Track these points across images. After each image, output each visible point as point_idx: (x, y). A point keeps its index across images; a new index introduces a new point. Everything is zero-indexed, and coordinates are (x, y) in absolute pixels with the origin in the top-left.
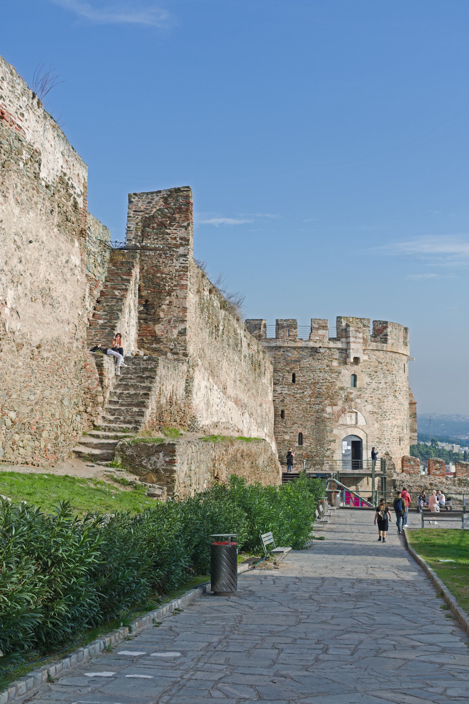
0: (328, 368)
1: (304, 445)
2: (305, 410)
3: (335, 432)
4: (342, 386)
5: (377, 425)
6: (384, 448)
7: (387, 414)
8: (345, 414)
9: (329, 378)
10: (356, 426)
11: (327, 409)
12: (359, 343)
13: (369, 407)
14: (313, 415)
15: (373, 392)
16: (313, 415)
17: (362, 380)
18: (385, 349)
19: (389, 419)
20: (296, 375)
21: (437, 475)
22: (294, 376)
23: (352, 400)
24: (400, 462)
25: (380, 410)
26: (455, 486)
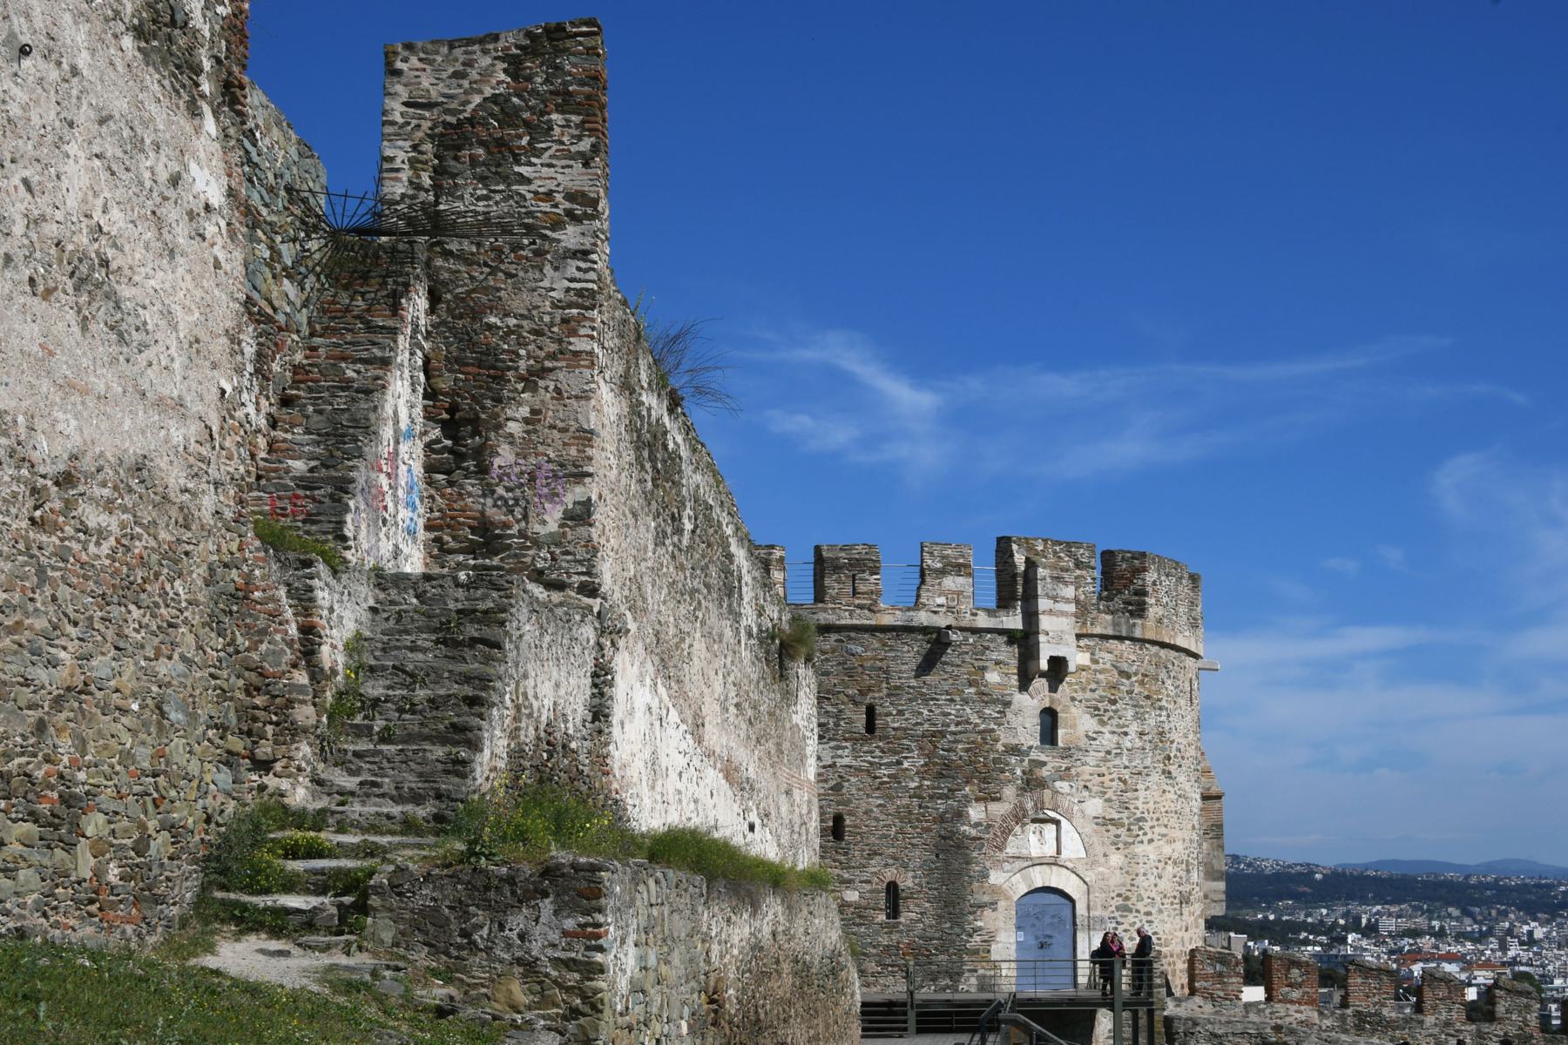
0: (972, 690)
1: (902, 920)
2: (905, 816)
3: (996, 878)
5: (1116, 859)
7: (1147, 826)
8: (1024, 824)
9: (975, 719)
10: (1054, 862)
11: (971, 811)
12: (1063, 614)
13: (1095, 806)
14: (928, 830)
15: (1105, 761)
16: (928, 830)
17: (1074, 726)
18: (1138, 633)
19: (1150, 841)
21: (1292, 1002)
22: (871, 712)
23: (1042, 784)
24: (1182, 966)
26: (1345, 1031)
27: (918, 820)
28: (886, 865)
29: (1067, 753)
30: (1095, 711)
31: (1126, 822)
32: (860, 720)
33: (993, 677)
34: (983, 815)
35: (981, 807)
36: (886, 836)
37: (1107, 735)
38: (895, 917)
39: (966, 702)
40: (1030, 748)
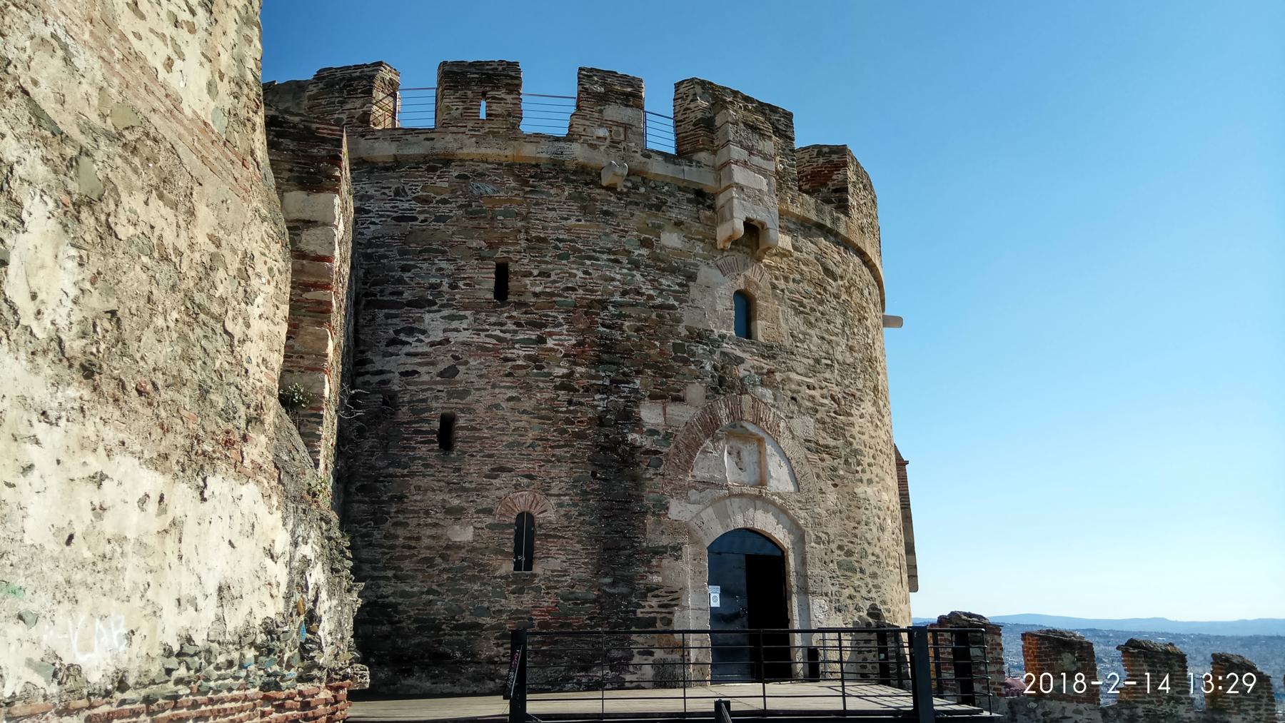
0: (645, 252)
2: (546, 414)
3: (678, 510)
4: (700, 326)
8: (716, 439)
9: (647, 289)
14: (580, 436)
16: (580, 436)
20: (513, 267)
22: (502, 273)
27: (568, 422)
28: (517, 487)
29: (769, 351)
30: (798, 308)
32: (488, 281)
34: (660, 420)
36: (519, 444)
38: (529, 567)
39: (636, 265)
40: (723, 337)
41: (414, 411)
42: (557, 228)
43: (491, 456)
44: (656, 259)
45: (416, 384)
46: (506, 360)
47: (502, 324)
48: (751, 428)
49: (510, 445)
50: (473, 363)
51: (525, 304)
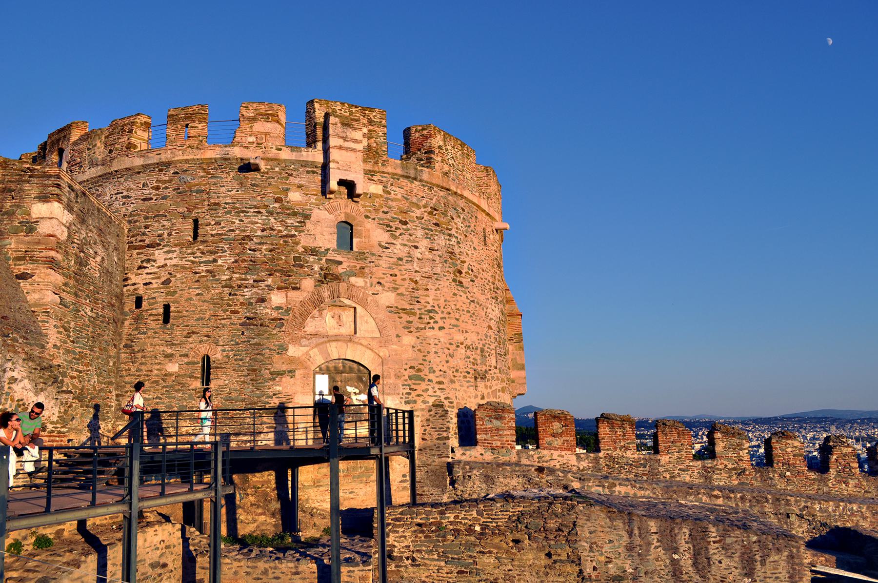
0: (277, 205)
2: (217, 302)
3: (293, 351)
4: (312, 245)
5: (408, 339)
6: (430, 392)
7: (437, 317)
10: (350, 339)
11: (273, 297)
13: (387, 298)
19: (441, 328)
21: (555, 449)
25: (418, 306)
29: (361, 256)
31: (418, 312)
33: (295, 196)
34: (284, 301)
35: (282, 294)
36: (202, 319)
37: (399, 246)
38: (208, 382)
40: (328, 250)
41: (150, 304)
42: (225, 197)
43: (187, 326)
44: (283, 208)
45: (151, 289)
46: (196, 273)
47: (194, 254)
48: (347, 302)
49: (198, 320)
50: (178, 276)
51: (206, 241)
